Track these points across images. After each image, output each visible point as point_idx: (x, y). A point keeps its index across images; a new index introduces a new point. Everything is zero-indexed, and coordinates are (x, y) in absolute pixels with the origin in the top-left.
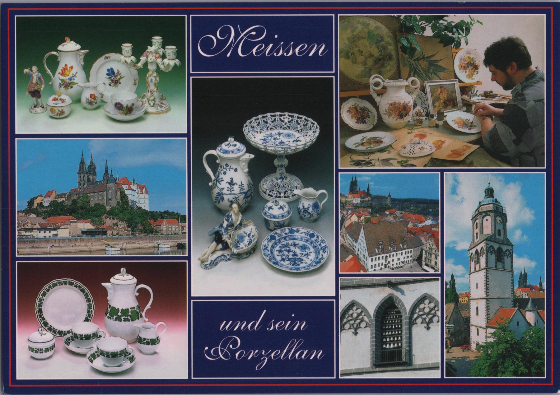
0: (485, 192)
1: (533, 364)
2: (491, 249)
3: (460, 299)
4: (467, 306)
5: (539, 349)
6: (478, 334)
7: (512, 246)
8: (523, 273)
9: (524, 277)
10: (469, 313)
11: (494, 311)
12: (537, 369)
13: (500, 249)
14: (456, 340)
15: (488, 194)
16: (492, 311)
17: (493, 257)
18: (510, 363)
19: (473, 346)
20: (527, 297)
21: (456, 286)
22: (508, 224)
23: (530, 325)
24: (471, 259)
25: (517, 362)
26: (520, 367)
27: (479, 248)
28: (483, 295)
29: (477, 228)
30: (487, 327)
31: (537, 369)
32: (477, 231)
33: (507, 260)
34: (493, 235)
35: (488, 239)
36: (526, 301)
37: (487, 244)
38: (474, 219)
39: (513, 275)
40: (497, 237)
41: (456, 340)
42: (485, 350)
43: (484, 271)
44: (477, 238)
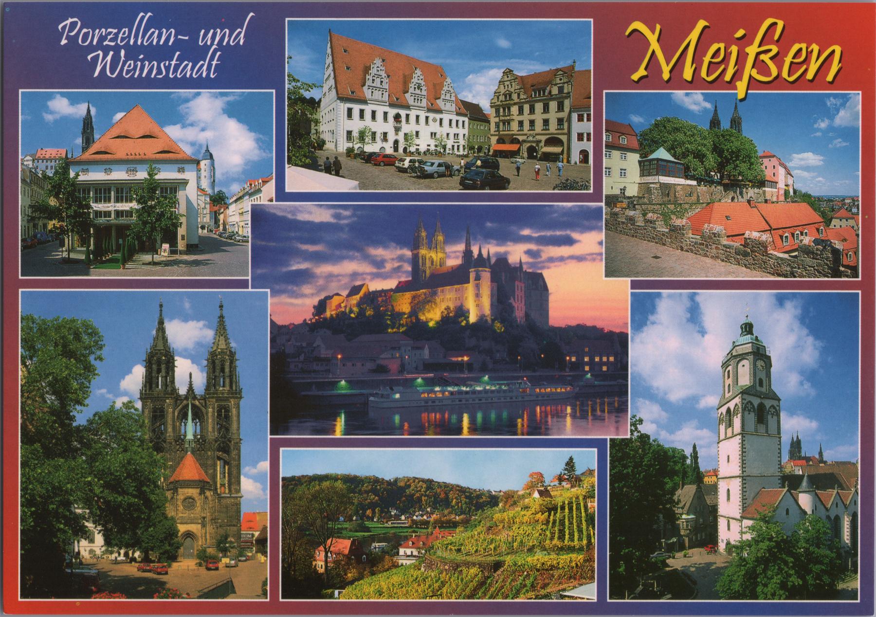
0: (742, 328)
1: (810, 572)
2: (749, 406)
3: (706, 479)
4: (714, 488)
5: (819, 548)
6: (729, 529)
7: (779, 400)
8: (795, 439)
9: (796, 445)
10: (717, 498)
11: (752, 495)
12: (816, 580)
13: (761, 406)
14: (697, 538)
15: (746, 331)
16: (750, 495)
17: (752, 418)
18: (776, 571)
19: (722, 546)
20: (801, 473)
21: (699, 460)
22: (772, 369)
23: (805, 513)
24: (721, 421)
25: (786, 569)
26: (790, 576)
27: (731, 405)
28: (737, 471)
29: (729, 377)
30: (743, 517)
31: (816, 580)
32: (729, 382)
33: (772, 421)
34: (752, 387)
35: (745, 392)
36: (801, 478)
37: (742, 399)
38: (725, 365)
40: (758, 388)
41: (697, 538)
42: (739, 551)
43: (740, 437)
44: (729, 392)
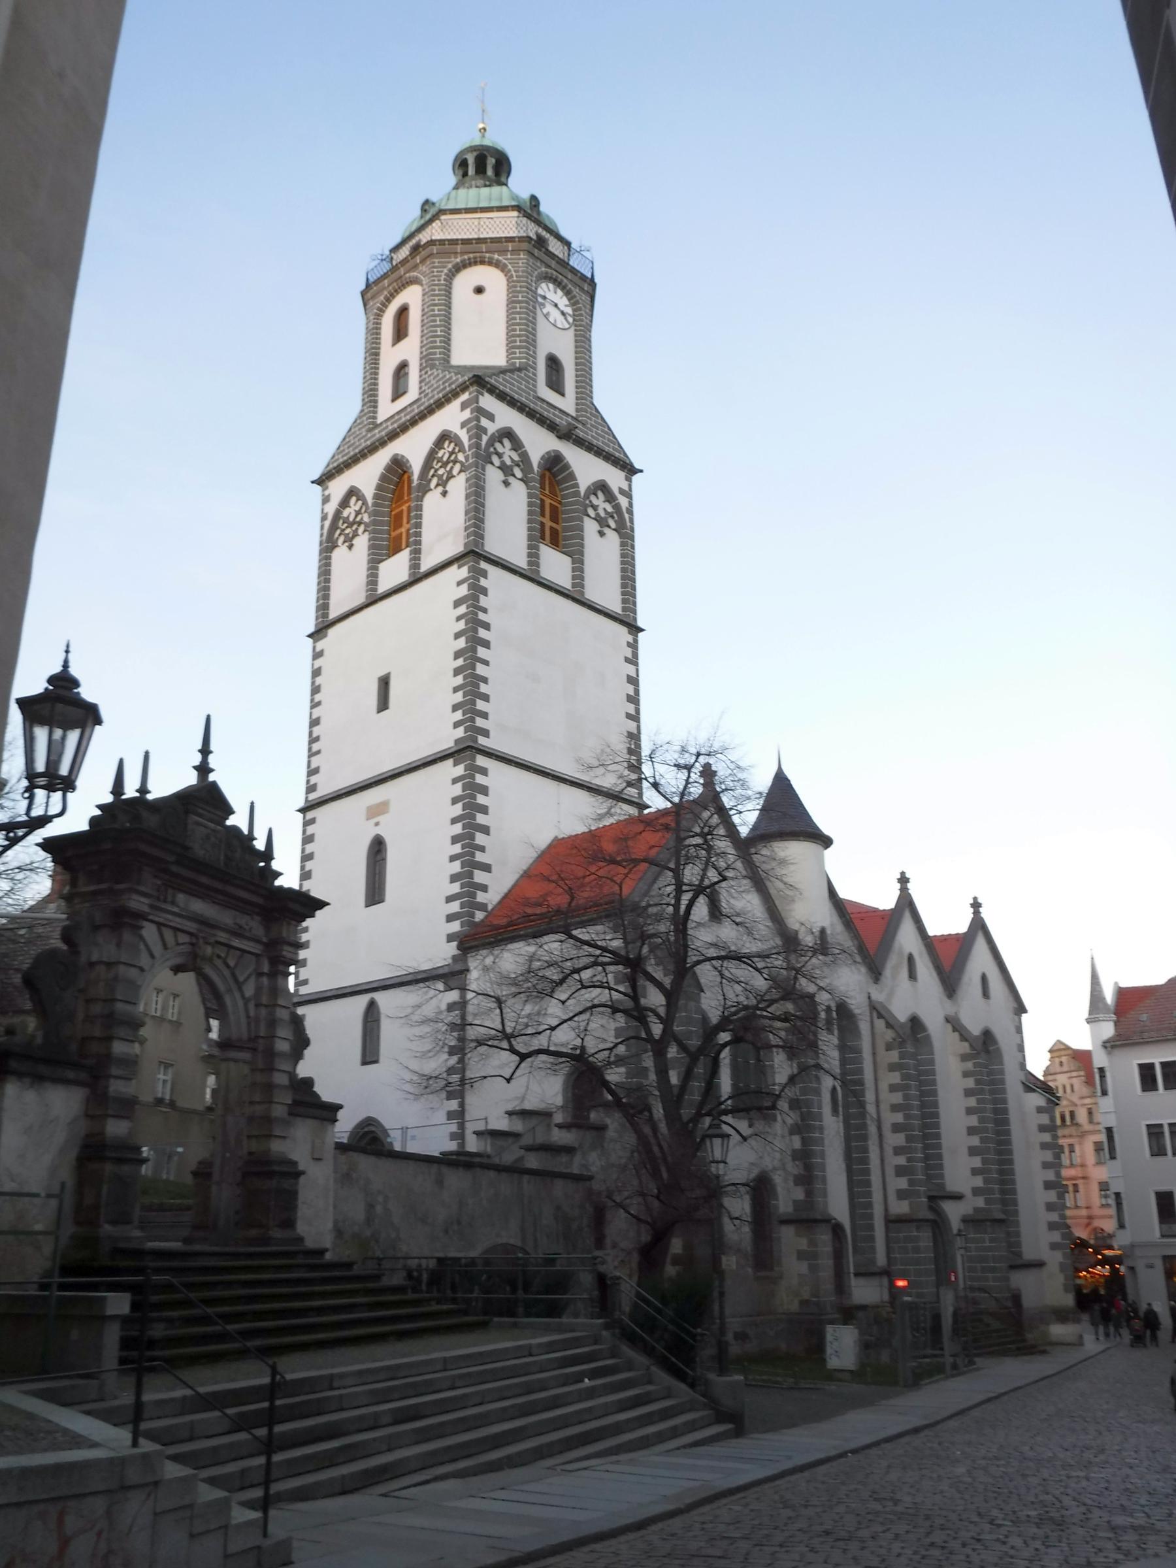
7: (630, 470)
33: (601, 550)
39: (634, 646)
